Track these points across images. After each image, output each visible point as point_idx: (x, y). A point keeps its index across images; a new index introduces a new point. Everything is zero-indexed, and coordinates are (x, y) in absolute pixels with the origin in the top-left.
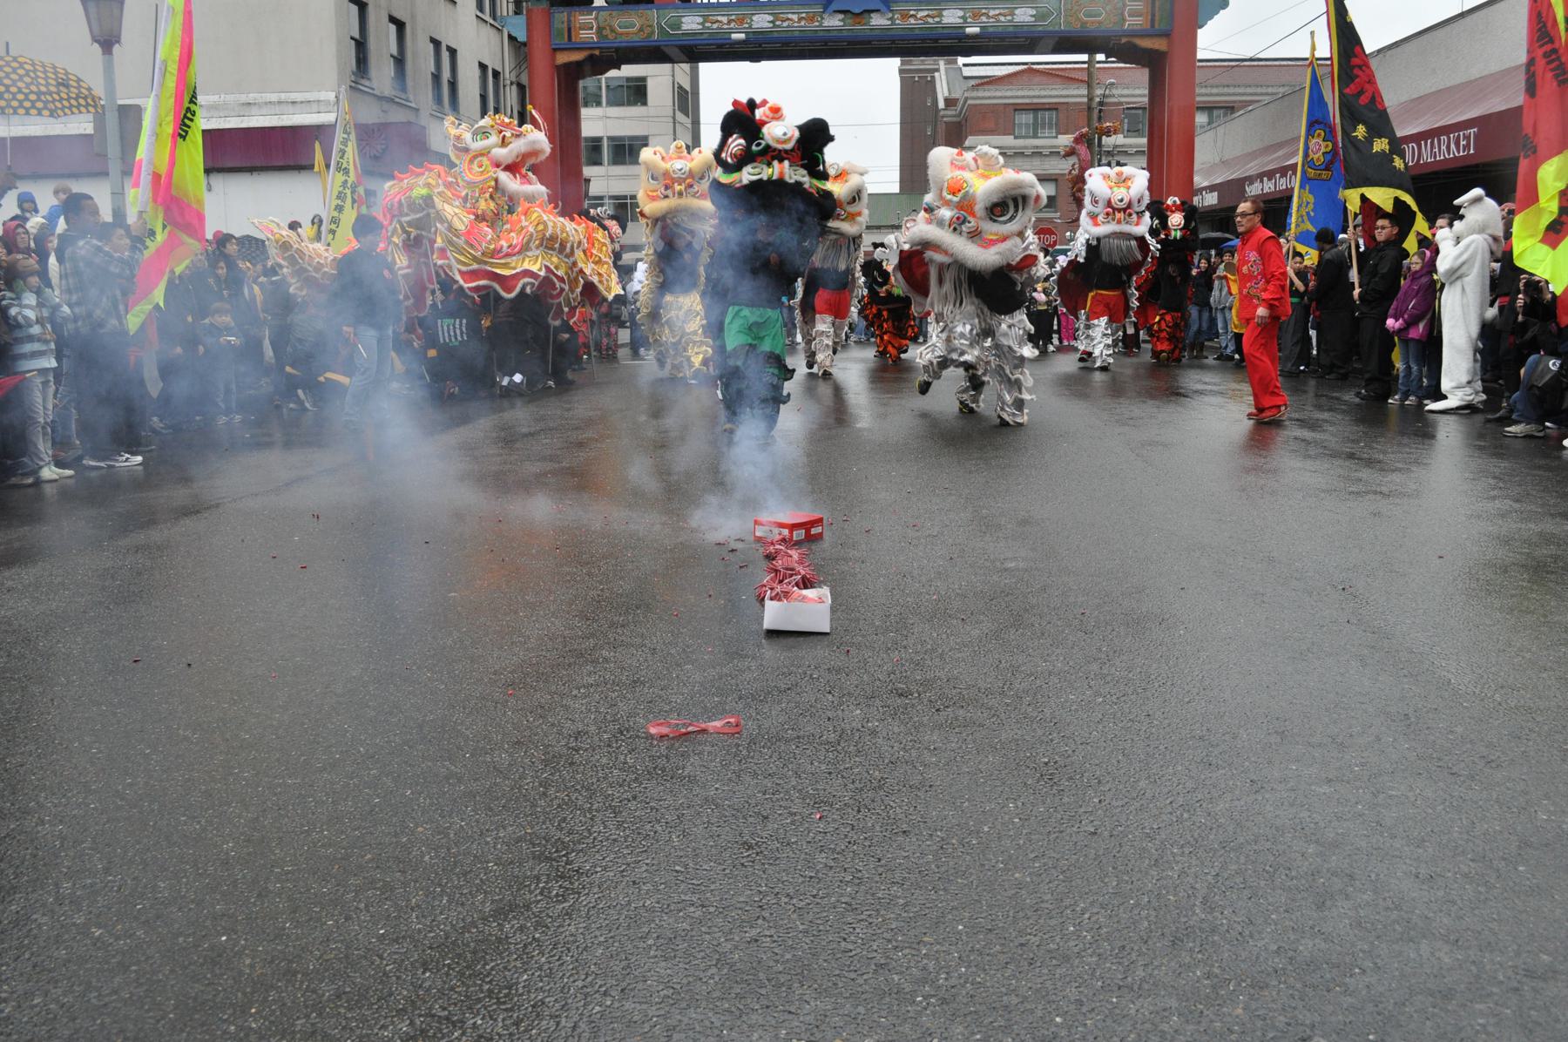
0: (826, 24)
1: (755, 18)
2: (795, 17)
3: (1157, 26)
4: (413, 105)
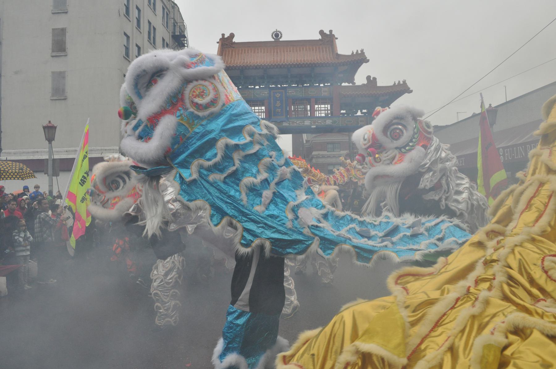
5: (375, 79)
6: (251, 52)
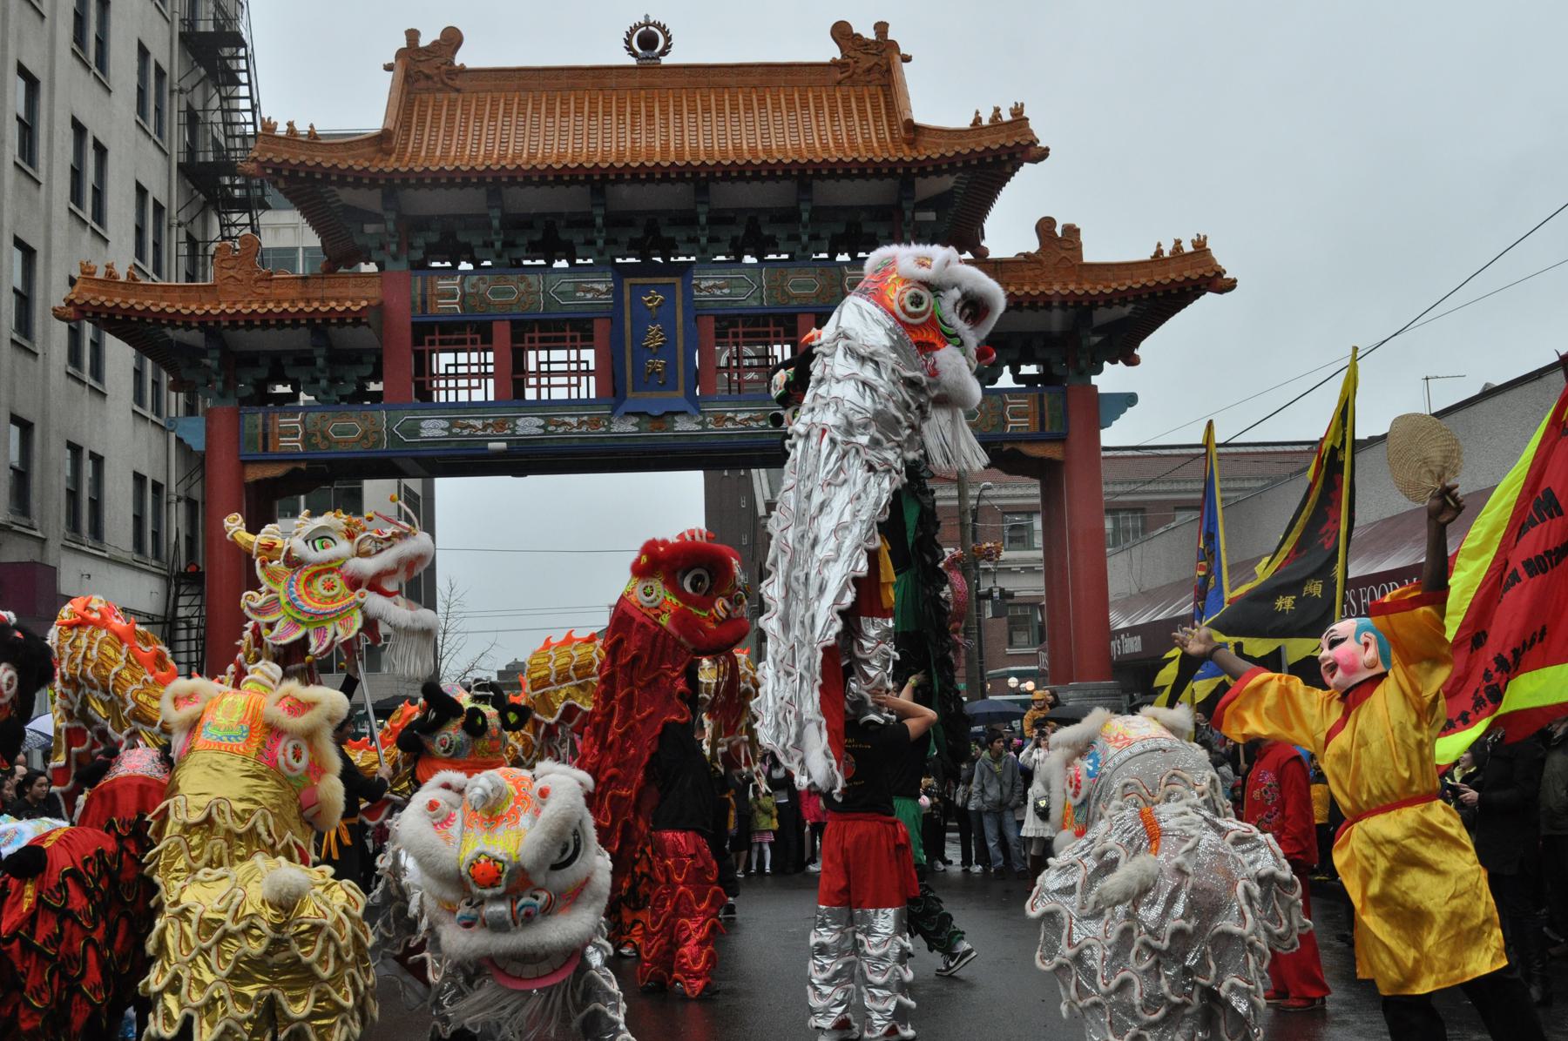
0: (615, 429)
1: (519, 422)
2: (574, 421)
3: (1047, 428)
4: (39, 534)
5: (1072, 232)
6: (536, 109)
